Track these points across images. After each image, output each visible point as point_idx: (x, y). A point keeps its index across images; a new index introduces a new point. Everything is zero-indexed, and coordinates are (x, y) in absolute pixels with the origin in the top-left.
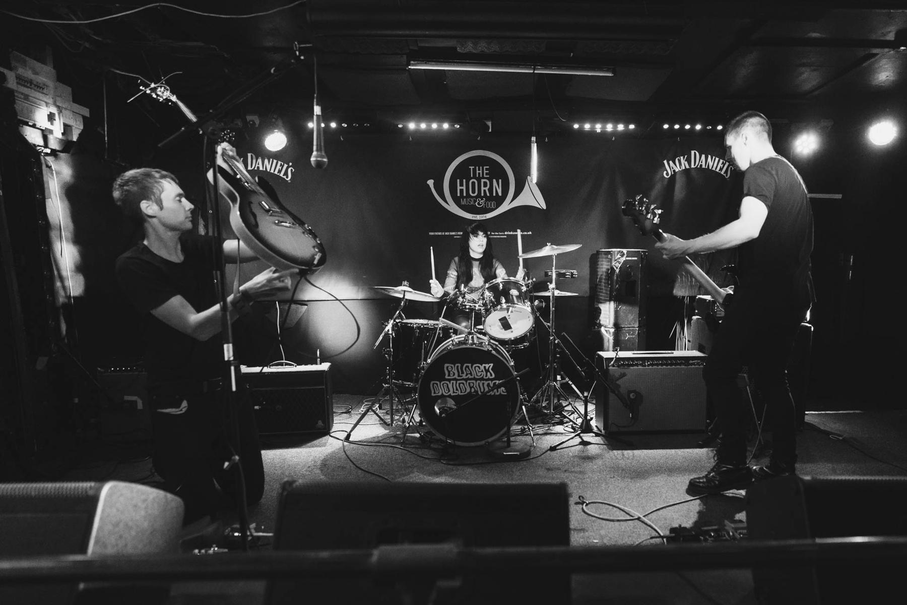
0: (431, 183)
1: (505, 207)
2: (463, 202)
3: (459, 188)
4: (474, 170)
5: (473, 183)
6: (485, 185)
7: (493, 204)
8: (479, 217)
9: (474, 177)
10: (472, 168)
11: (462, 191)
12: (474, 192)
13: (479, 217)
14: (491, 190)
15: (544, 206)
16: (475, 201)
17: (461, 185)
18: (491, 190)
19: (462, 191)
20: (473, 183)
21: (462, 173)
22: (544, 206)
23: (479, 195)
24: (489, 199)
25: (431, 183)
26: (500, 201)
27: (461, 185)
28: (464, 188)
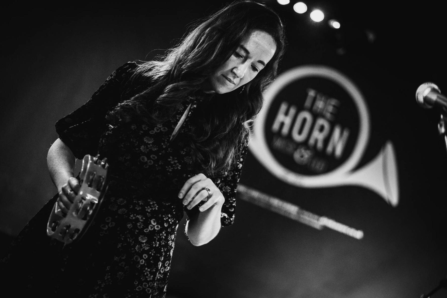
1: (339, 177)
2: (278, 143)
3: (281, 117)
4: (314, 100)
5: (305, 120)
7: (319, 165)
8: (292, 178)
9: (311, 110)
10: (312, 93)
11: (282, 124)
13: (292, 178)
14: (327, 141)
15: (392, 195)
16: (295, 149)
17: (286, 114)
18: (327, 141)
19: (282, 124)
20: (305, 120)
22: (392, 195)
23: (305, 144)
26: (332, 163)
27: (286, 114)
28: (288, 121)
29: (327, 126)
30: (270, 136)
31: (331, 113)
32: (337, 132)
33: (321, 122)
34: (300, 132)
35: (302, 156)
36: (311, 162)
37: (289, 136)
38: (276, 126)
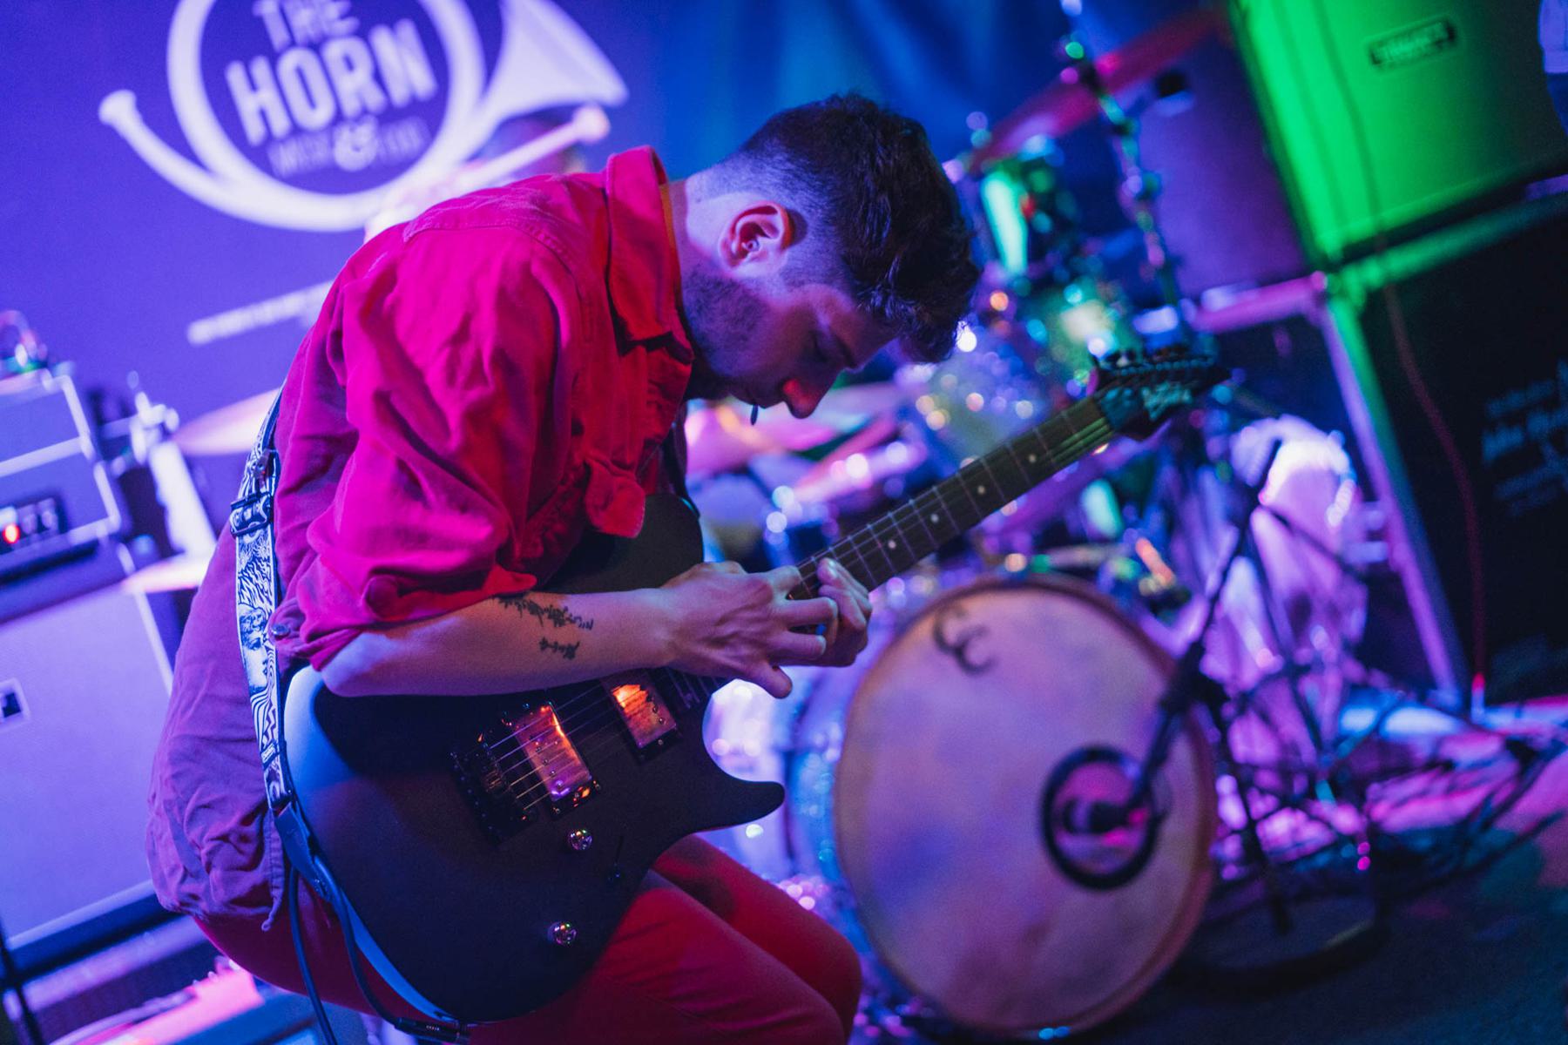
0: (119, 110)
2: (288, 158)
3: (248, 105)
6: (349, 64)
7: (406, 137)
11: (263, 114)
12: (312, 103)
14: (378, 77)
16: (332, 144)
17: (253, 86)
18: (378, 77)
19: (263, 114)
21: (236, 36)
23: (339, 118)
24: (389, 116)
25: (119, 110)
26: (430, 113)
27: (253, 86)
28: (267, 96)
29: (356, 48)
30: (259, 156)
31: (343, 17)
32: (382, 39)
33: (334, 51)
34: (312, 103)
35: (355, 148)
36: (385, 146)
37: (296, 131)
38: (254, 131)
